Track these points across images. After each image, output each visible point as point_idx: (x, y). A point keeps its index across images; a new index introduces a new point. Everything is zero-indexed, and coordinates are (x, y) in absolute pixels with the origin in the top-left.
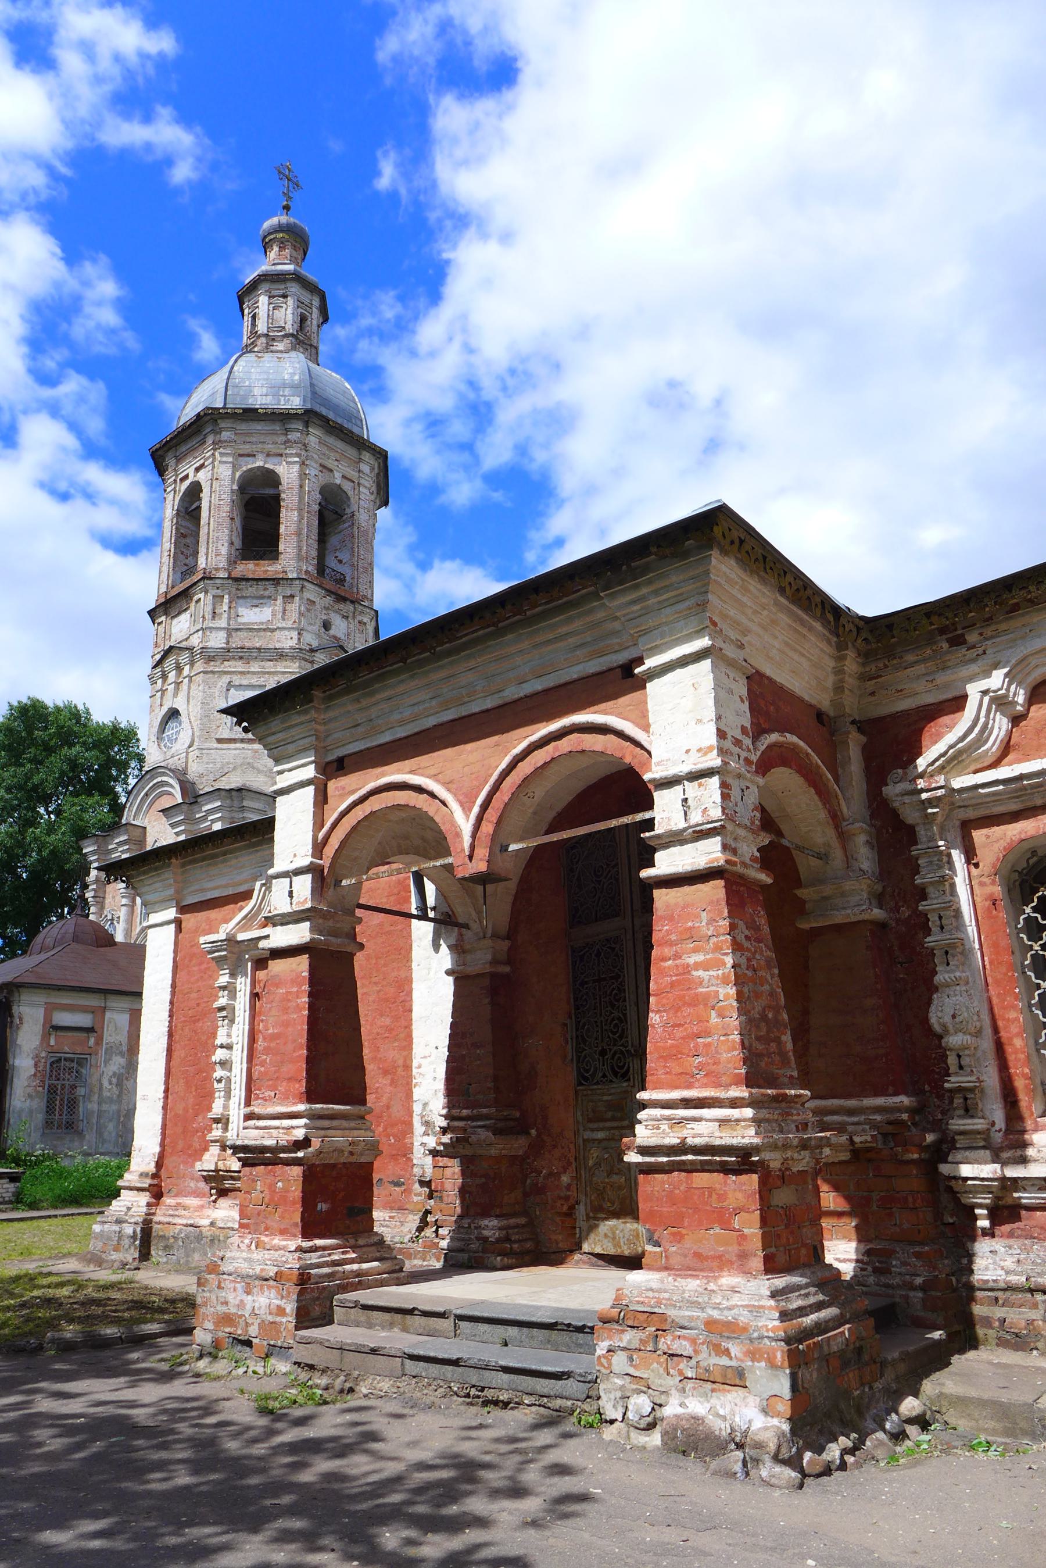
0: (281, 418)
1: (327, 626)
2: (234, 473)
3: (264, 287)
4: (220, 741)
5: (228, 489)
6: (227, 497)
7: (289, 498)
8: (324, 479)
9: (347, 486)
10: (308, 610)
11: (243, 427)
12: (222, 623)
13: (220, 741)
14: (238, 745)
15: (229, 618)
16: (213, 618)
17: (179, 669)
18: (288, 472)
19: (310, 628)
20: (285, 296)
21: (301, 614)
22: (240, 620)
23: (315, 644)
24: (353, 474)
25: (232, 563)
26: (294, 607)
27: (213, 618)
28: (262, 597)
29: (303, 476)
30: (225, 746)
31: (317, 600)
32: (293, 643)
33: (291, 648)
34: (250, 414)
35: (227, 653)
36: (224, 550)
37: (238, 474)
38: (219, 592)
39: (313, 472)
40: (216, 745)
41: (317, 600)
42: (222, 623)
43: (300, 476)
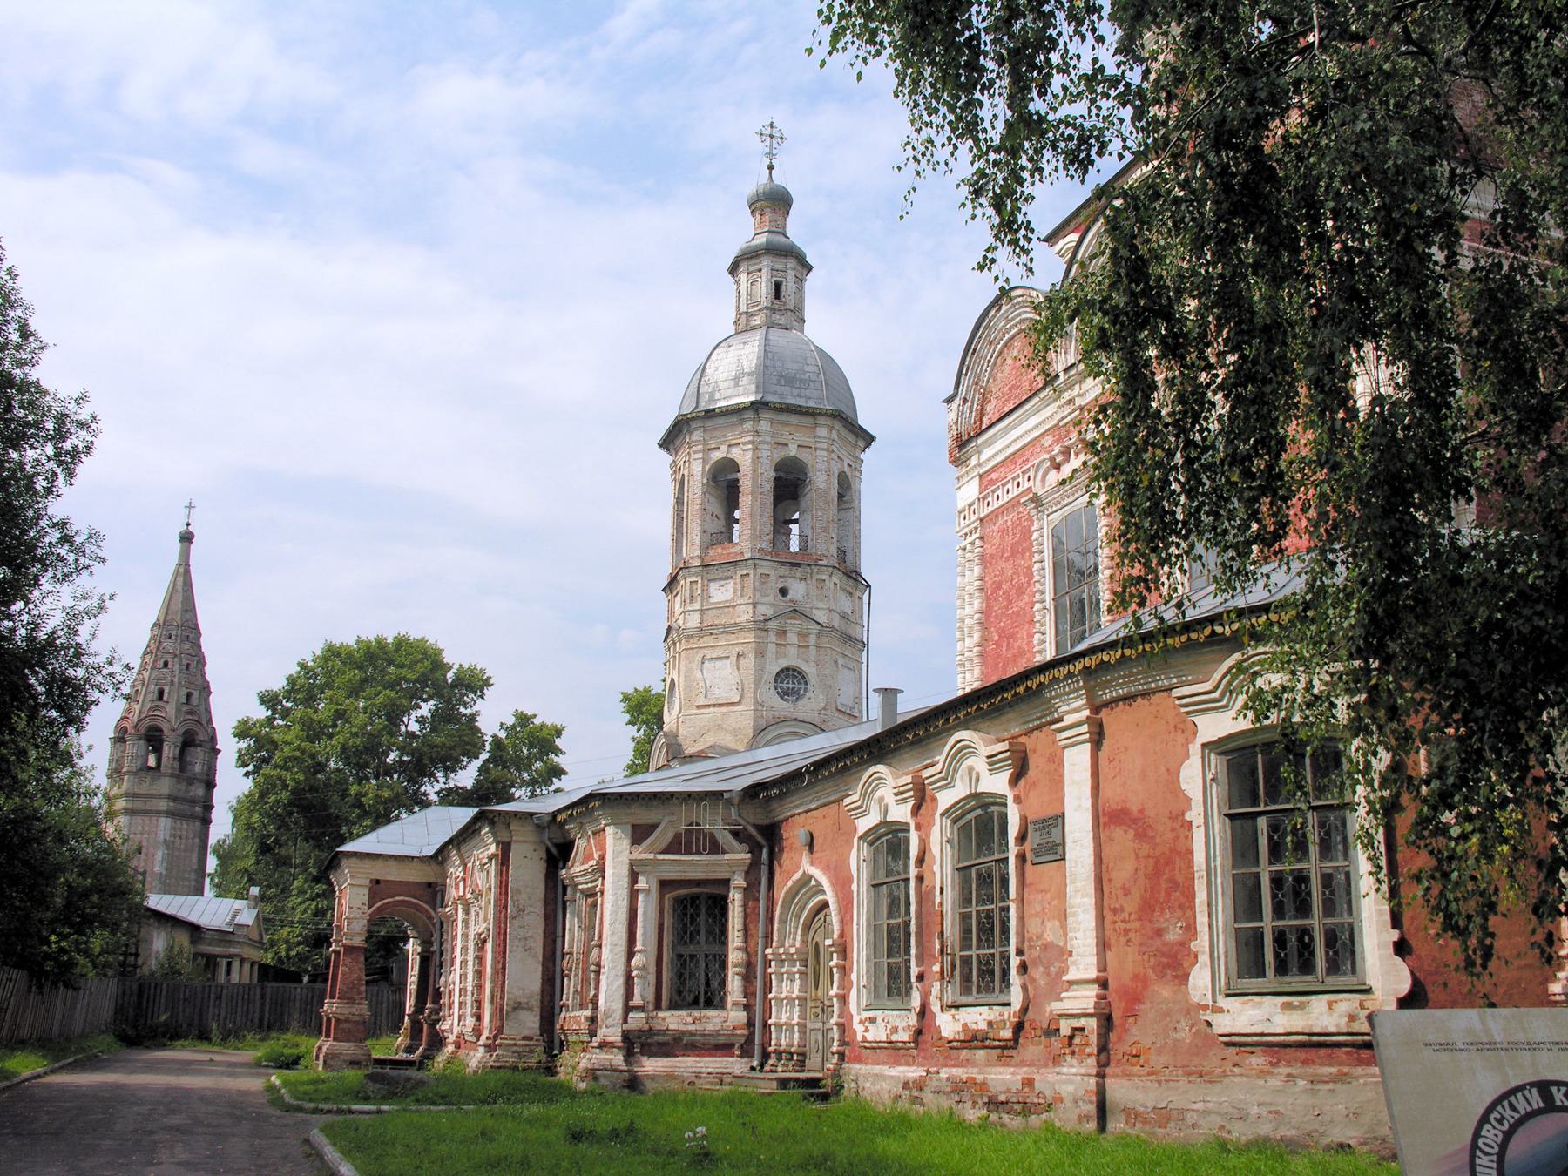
0: (737, 411)
1: (784, 592)
2: (704, 468)
3: (743, 268)
4: (698, 707)
5: (699, 484)
6: (698, 491)
7: (745, 484)
8: (778, 455)
9: (804, 456)
10: (763, 583)
11: (709, 423)
12: (697, 606)
13: (698, 707)
14: (712, 710)
15: (702, 601)
16: (691, 602)
17: (674, 644)
18: (743, 457)
19: (765, 599)
20: (760, 271)
21: (755, 589)
22: (712, 600)
23: (770, 612)
24: (807, 440)
25: (705, 549)
26: (749, 582)
27: (691, 602)
28: (727, 578)
29: (756, 459)
30: (703, 711)
31: (772, 573)
32: (748, 617)
33: (748, 621)
34: (710, 414)
35: (704, 631)
36: (697, 540)
37: (708, 467)
38: (694, 579)
39: (765, 454)
40: (695, 711)
41: (772, 573)
42: (697, 606)
43: (753, 461)
